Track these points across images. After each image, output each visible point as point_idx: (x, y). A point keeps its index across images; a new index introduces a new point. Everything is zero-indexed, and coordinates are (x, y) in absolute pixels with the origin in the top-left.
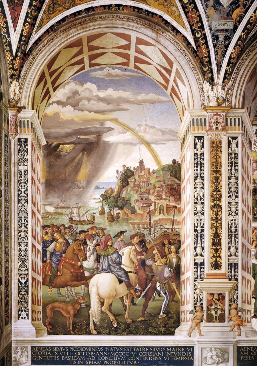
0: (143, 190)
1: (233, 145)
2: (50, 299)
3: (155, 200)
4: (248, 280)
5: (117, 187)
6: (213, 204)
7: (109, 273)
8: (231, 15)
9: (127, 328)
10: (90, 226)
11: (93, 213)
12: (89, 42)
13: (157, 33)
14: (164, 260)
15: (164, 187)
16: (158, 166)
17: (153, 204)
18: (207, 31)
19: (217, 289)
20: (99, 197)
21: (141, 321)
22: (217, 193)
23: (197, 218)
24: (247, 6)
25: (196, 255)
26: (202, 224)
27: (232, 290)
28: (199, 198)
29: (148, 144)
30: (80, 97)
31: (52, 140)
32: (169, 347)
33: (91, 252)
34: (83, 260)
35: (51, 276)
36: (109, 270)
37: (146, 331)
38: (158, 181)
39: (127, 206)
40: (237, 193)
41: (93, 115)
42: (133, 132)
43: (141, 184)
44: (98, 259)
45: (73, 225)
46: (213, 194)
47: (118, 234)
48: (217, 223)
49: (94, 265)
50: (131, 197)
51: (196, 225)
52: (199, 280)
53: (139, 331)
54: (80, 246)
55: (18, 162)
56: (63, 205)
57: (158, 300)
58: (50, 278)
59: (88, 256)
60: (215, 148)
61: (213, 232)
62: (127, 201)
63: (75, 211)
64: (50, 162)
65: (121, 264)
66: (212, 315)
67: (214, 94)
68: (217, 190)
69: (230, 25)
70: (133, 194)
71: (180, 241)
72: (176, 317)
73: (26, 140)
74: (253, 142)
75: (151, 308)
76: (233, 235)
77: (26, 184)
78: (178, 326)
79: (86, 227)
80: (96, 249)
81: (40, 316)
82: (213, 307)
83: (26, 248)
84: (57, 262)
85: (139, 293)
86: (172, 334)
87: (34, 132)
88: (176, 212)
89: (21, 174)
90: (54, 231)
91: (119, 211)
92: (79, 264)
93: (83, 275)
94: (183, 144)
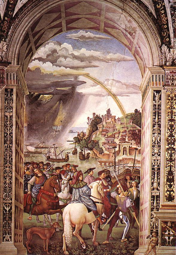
0: (109, 134)
2: (29, 224)
3: (120, 143)
5: (88, 131)
6: (167, 147)
7: (80, 203)
9: (95, 250)
10: (64, 163)
11: (67, 153)
12: (66, 9)
14: (125, 193)
16: (123, 115)
17: (118, 146)
19: (170, 218)
20: (73, 140)
21: (106, 244)
22: (171, 138)
23: (155, 158)
25: (153, 189)
26: (159, 163)
28: (156, 142)
29: (114, 96)
30: (58, 55)
31: (34, 91)
33: (65, 185)
34: (58, 192)
36: (79, 200)
37: (110, 253)
39: (96, 147)
41: (68, 70)
43: (108, 129)
44: (71, 191)
45: (50, 162)
46: (168, 139)
47: (88, 171)
48: (171, 163)
49: (68, 196)
51: (153, 164)
52: (155, 210)
54: (56, 180)
55: (5, 109)
56: (42, 146)
57: (120, 227)
59: (62, 189)
60: (170, 100)
61: (167, 170)
63: (52, 150)
64: (32, 109)
65: (90, 196)
67: (171, 55)
71: (140, 177)
73: (12, 90)
75: (115, 233)
77: (11, 128)
79: (61, 164)
80: (69, 182)
81: (21, 238)
82: (167, 233)
83: (10, 182)
85: (105, 220)
87: (19, 84)
88: (137, 154)
89: (7, 119)
90: (34, 167)
91: (89, 151)
93: (58, 204)
94: (143, 96)
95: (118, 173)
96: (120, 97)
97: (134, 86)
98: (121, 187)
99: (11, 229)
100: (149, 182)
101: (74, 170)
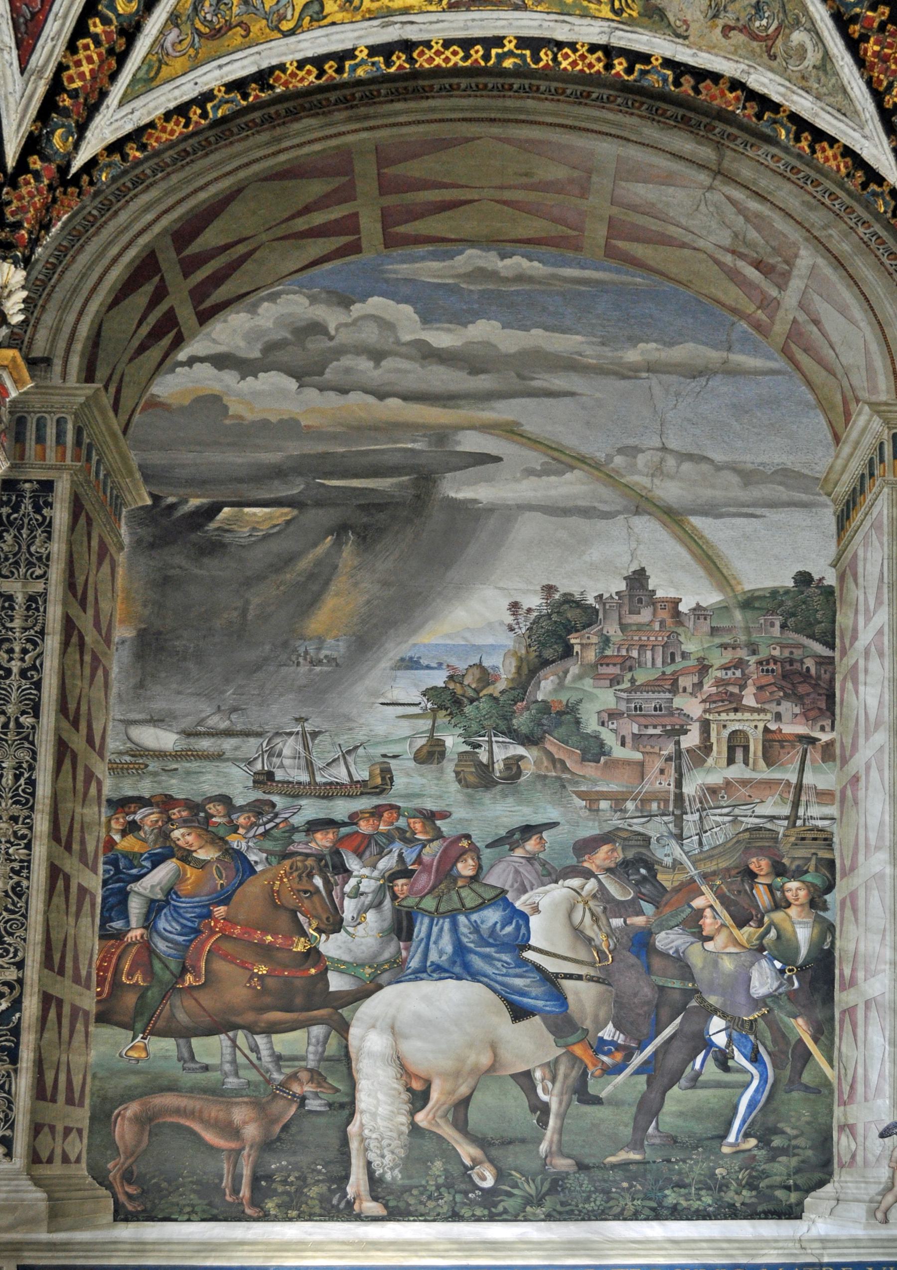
0: (642, 677)
3: (705, 711)
10: (364, 803)
11: (384, 756)
15: (752, 667)
20: (415, 696)
21: (624, 1165)
34: (319, 930)
35: (147, 989)
38: (724, 646)
39: (562, 730)
42: (596, 473)
43: (635, 654)
47: (511, 833)
50: (581, 701)
53: (611, 1203)
54: (310, 876)
58: (142, 997)
62: (560, 713)
63: (289, 747)
70: (590, 690)
79: (341, 809)
84: (181, 939)
91: (520, 750)
92: (300, 946)
95: (696, 846)
96: (710, 520)
98: (718, 907)
99: (10, 1102)
101: (425, 832)
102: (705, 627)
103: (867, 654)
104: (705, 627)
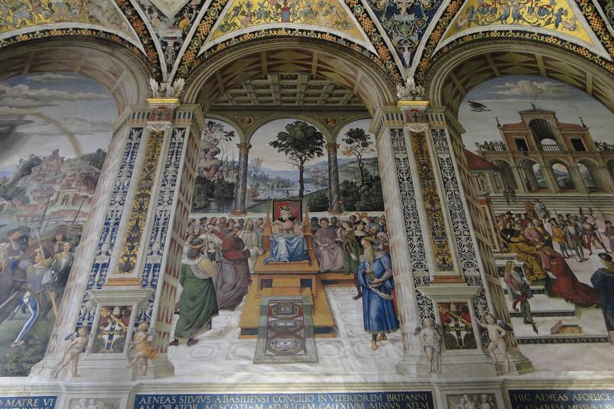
1: (179, 134)
4: (172, 287)
5: (14, 176)
6: (139, 193)
8: (178, 25)
13: (113, 49)
17: (55, 195)
18: (154, 38)
19: (120, 300)
23: (112, 209)
24: (193, 18)
27: (144, 301)
28: (121, 187)
29: (71, 135)
32: (11, 399)
38: (72, 170)
40: (175, 181)
41: (14, 110)
51: (109, 216)
57: (20, 318)
62: (21, 191)
66: (102, 341)
68: (149, 178)
69: (178, 33)
71: (80, 236)
72: (42, 345)
74: (203, 132)
76: (159, 229)
78: (39, 360)
82: (108, 328)
86: (24, 373)
91: (6, 202)
94: (115, 134)
97: (103, 123)
98: (42, 252)
100: (95, 242)
102: (68, 164)
103: (110, 171)
104: (68, 164)
